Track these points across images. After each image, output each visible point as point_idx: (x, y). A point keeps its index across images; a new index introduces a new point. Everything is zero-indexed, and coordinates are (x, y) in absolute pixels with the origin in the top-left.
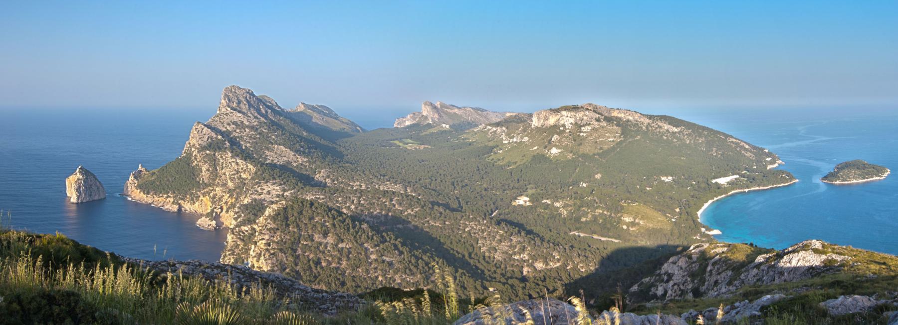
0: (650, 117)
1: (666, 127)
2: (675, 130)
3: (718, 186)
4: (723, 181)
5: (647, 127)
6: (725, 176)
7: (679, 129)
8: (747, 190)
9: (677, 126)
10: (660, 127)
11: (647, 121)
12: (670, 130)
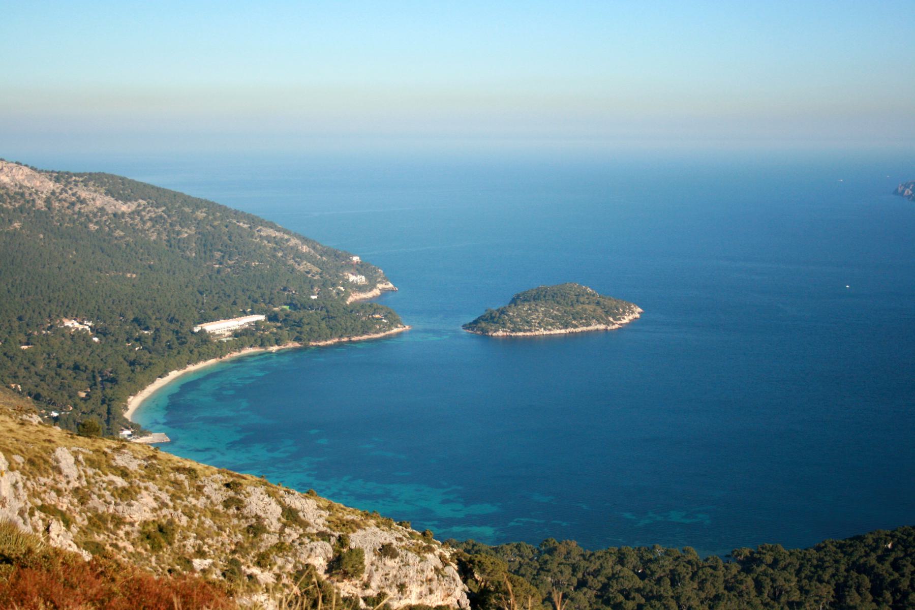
0: (58, 177)
1: (100, 200)
2: (124, 208)
3: (204, 338)
4: (221, 328)
5: (48, 201)
6: (227, 317)
7: (133, 206)
8: (275, 348)
9: (126, 199)
10: (83, 201)
11: (51, 185)
12: (110, 210)
